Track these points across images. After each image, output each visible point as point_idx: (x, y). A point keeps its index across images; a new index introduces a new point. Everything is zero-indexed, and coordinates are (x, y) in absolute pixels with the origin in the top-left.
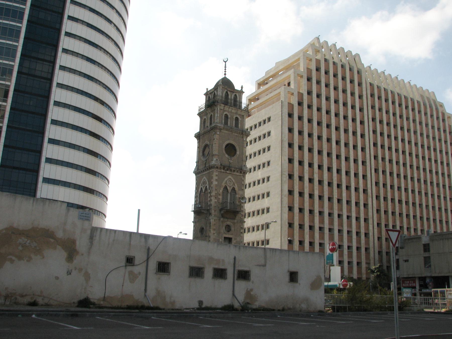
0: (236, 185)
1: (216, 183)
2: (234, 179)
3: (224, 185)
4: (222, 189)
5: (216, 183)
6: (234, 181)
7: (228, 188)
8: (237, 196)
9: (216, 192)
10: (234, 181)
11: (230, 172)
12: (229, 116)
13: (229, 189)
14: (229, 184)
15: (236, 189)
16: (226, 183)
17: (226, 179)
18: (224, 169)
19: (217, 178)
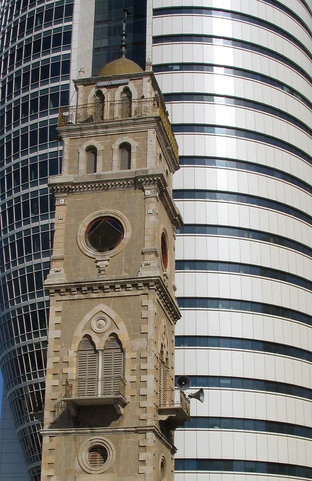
0: (122, 325)
1: (58, 333)
2: (114, 309)
3: (80, 334)
4: (75, 347)
5: (58, 333)
6: (113, 315)
7: (96, 339)
8: (128, 355)
9: (57, 359)
10: (113, 315)
11: (101, 295)
12: (100, 148)
13: (99, 343)
14: (99, 326)
15: (124, 336)
16: (89, 326)
17: (87, 317)
18: (79, 289)
19: (58, 319)
